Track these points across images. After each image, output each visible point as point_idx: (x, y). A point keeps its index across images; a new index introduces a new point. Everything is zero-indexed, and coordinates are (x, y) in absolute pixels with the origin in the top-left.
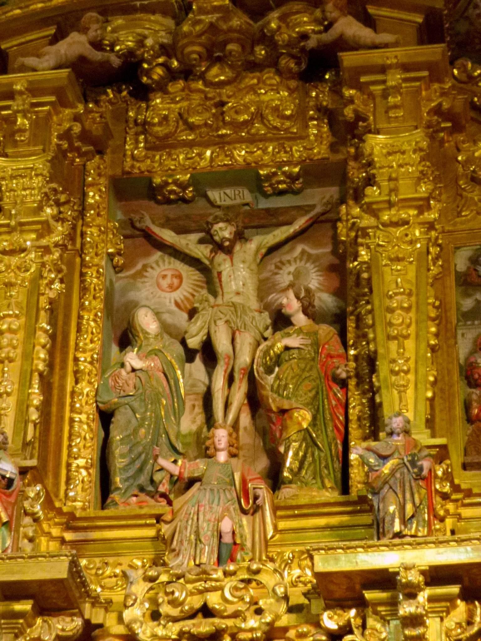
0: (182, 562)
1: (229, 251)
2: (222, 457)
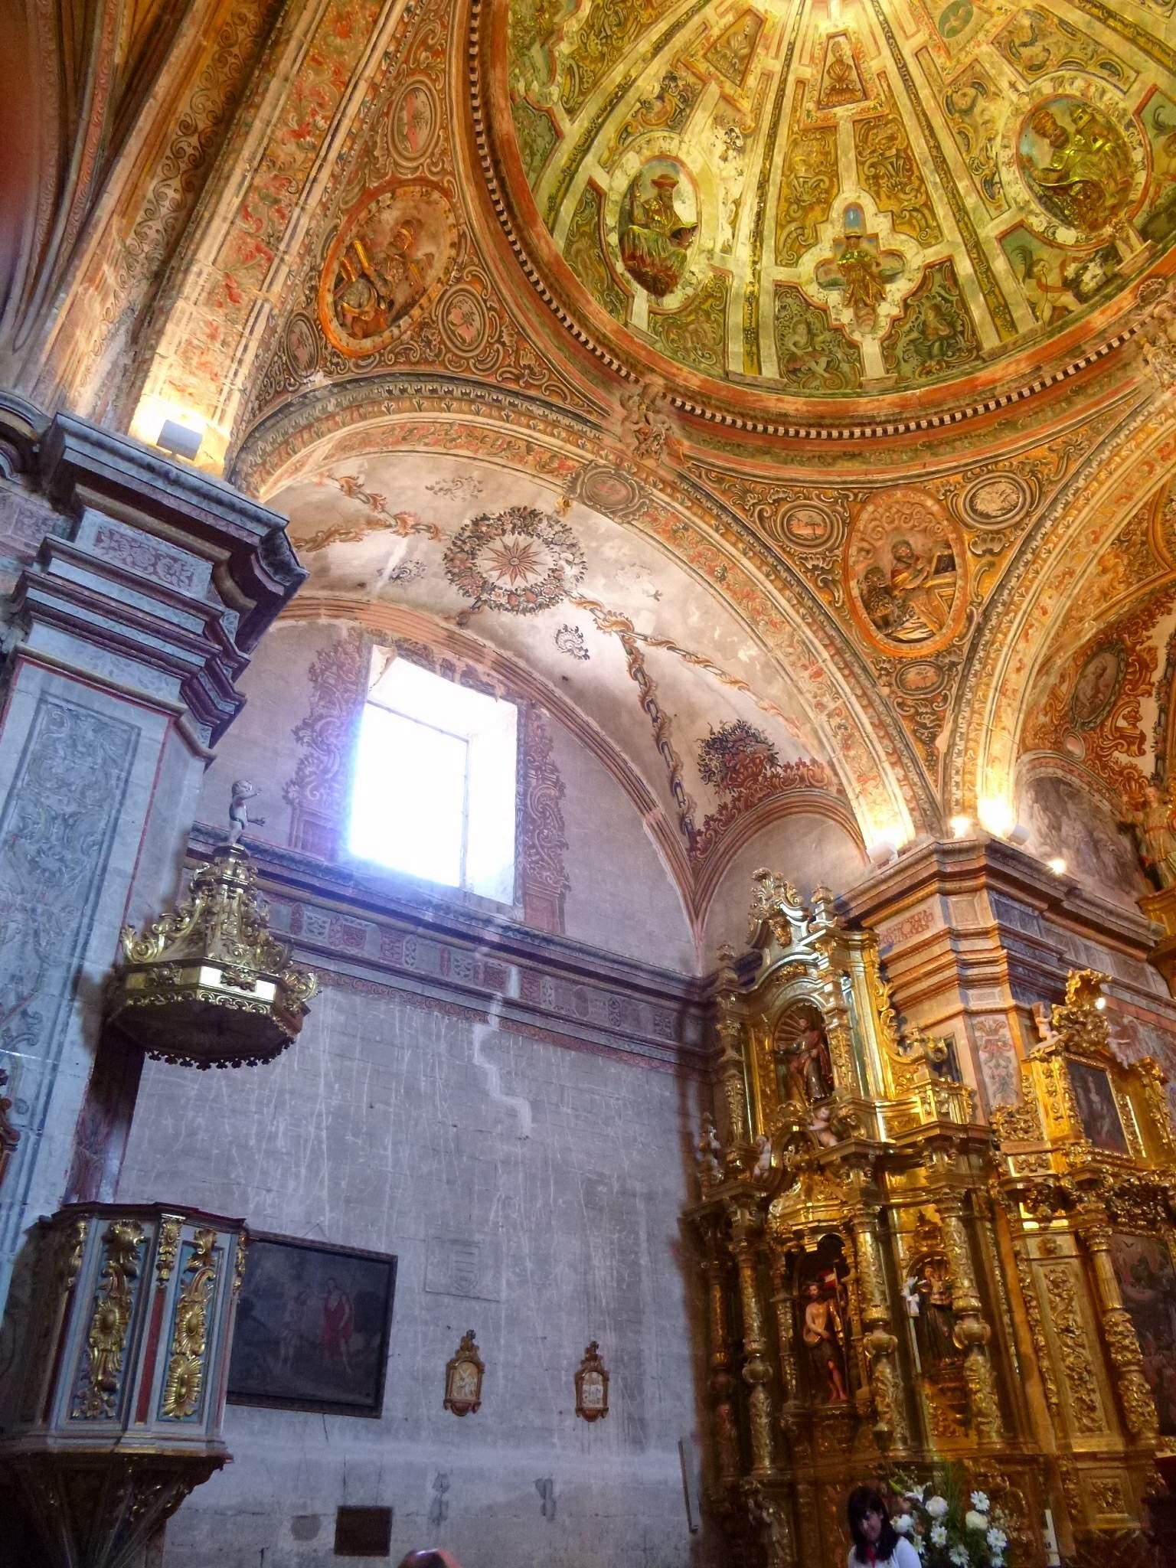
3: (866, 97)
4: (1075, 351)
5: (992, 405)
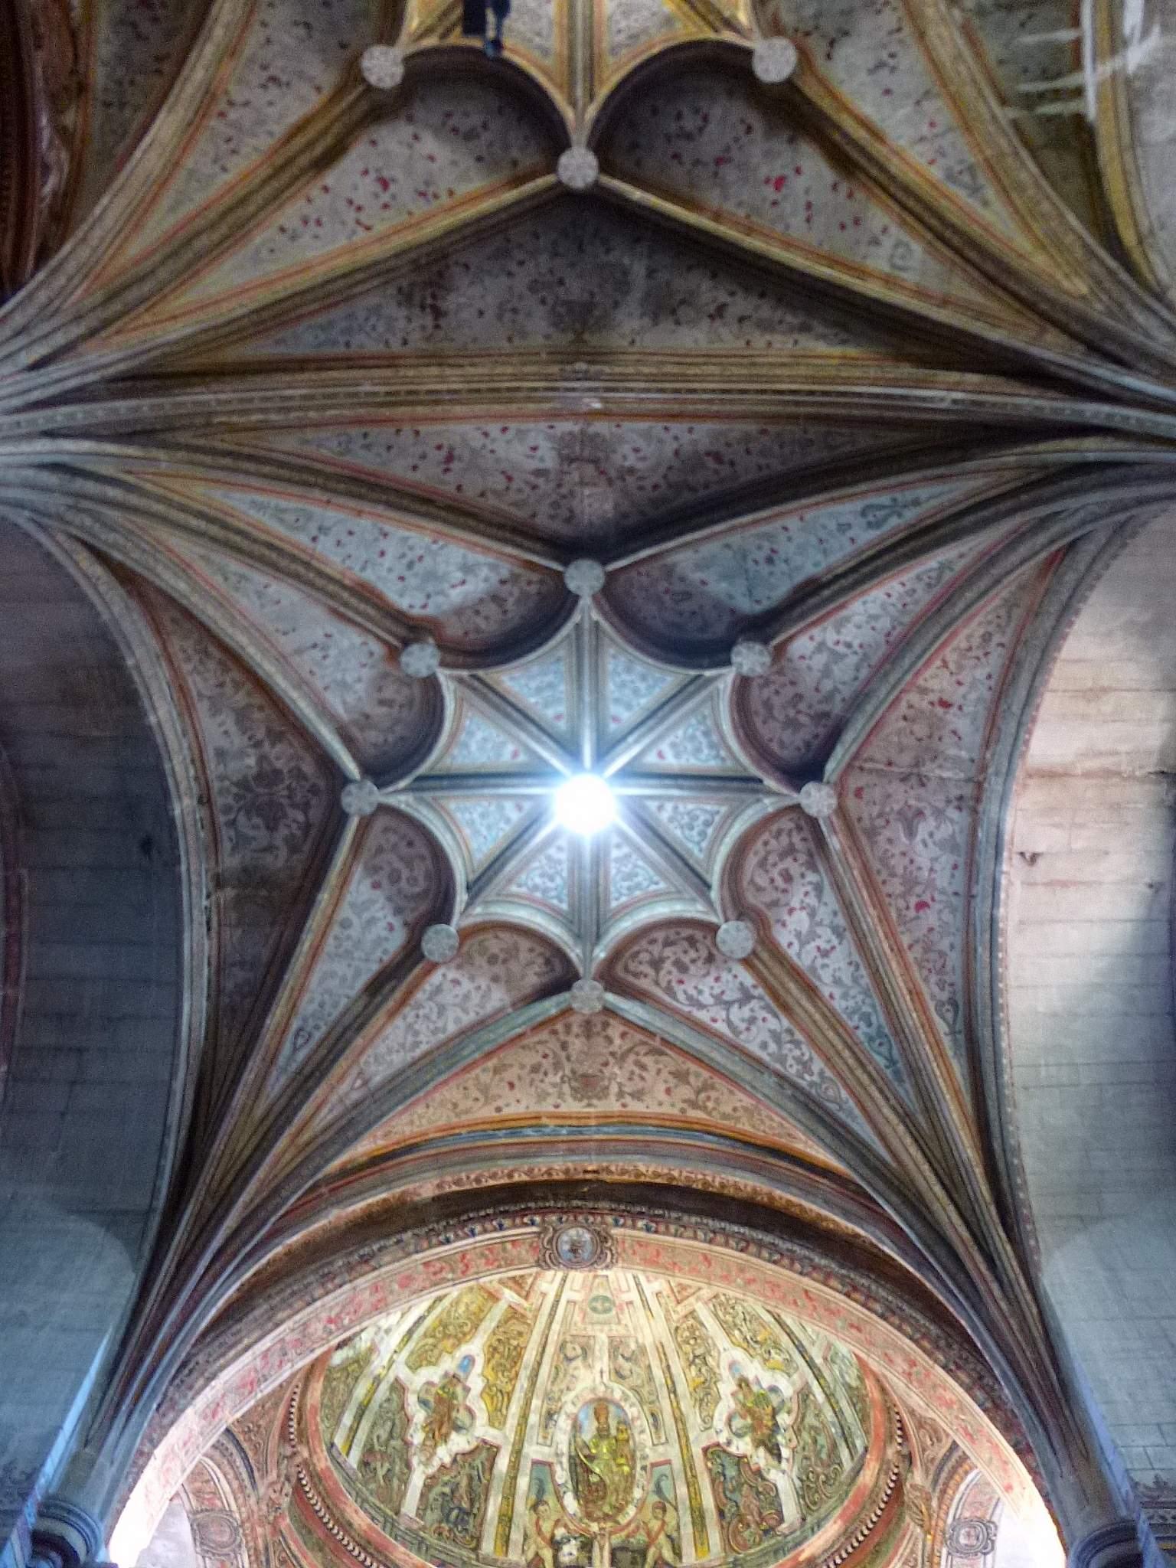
3: (526, 1298)
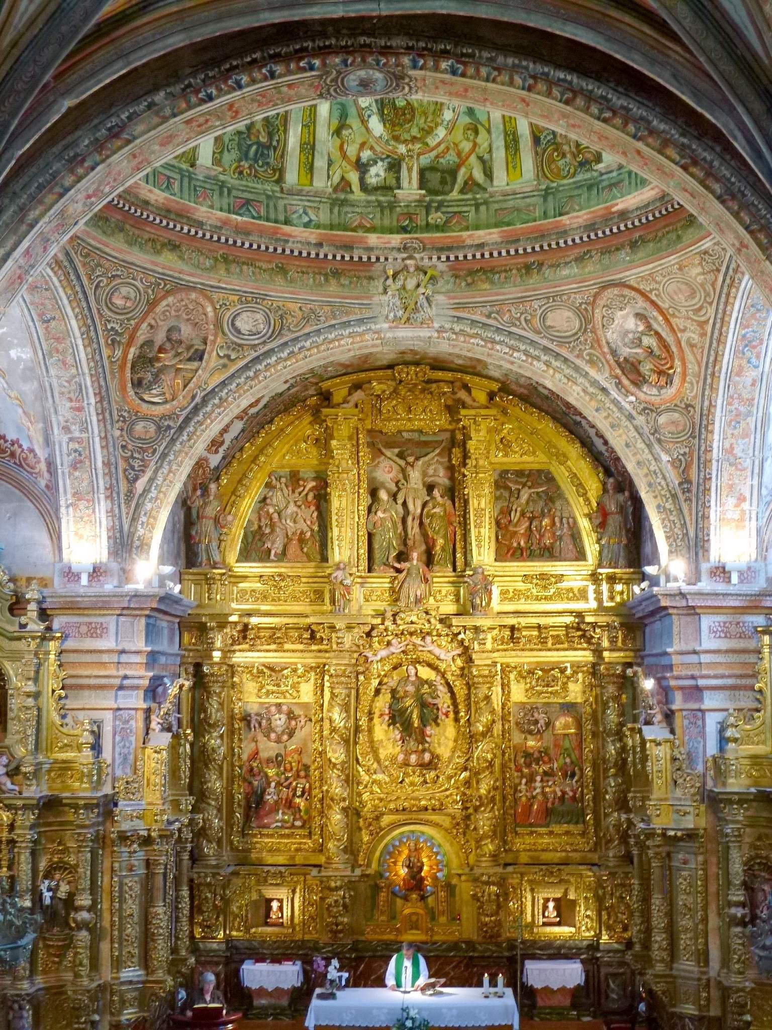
0: (402, 604)
1: (412, 466)
2: (415, 562)
4: (349, 247)
5: (279, 251)
